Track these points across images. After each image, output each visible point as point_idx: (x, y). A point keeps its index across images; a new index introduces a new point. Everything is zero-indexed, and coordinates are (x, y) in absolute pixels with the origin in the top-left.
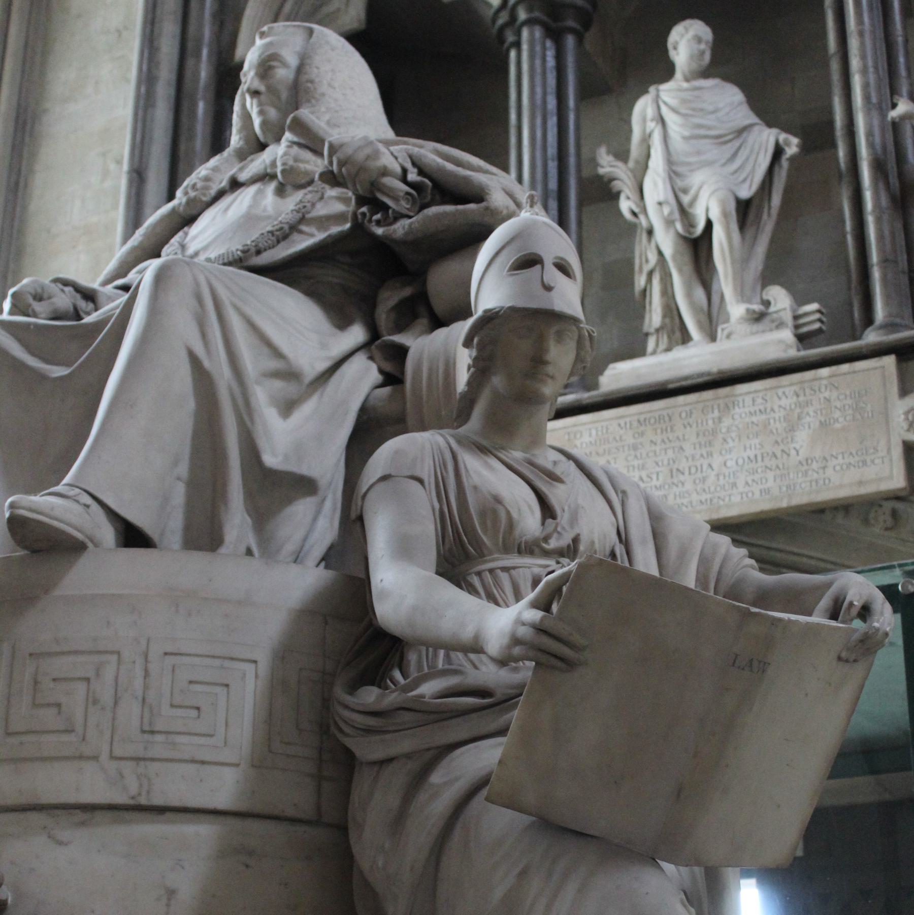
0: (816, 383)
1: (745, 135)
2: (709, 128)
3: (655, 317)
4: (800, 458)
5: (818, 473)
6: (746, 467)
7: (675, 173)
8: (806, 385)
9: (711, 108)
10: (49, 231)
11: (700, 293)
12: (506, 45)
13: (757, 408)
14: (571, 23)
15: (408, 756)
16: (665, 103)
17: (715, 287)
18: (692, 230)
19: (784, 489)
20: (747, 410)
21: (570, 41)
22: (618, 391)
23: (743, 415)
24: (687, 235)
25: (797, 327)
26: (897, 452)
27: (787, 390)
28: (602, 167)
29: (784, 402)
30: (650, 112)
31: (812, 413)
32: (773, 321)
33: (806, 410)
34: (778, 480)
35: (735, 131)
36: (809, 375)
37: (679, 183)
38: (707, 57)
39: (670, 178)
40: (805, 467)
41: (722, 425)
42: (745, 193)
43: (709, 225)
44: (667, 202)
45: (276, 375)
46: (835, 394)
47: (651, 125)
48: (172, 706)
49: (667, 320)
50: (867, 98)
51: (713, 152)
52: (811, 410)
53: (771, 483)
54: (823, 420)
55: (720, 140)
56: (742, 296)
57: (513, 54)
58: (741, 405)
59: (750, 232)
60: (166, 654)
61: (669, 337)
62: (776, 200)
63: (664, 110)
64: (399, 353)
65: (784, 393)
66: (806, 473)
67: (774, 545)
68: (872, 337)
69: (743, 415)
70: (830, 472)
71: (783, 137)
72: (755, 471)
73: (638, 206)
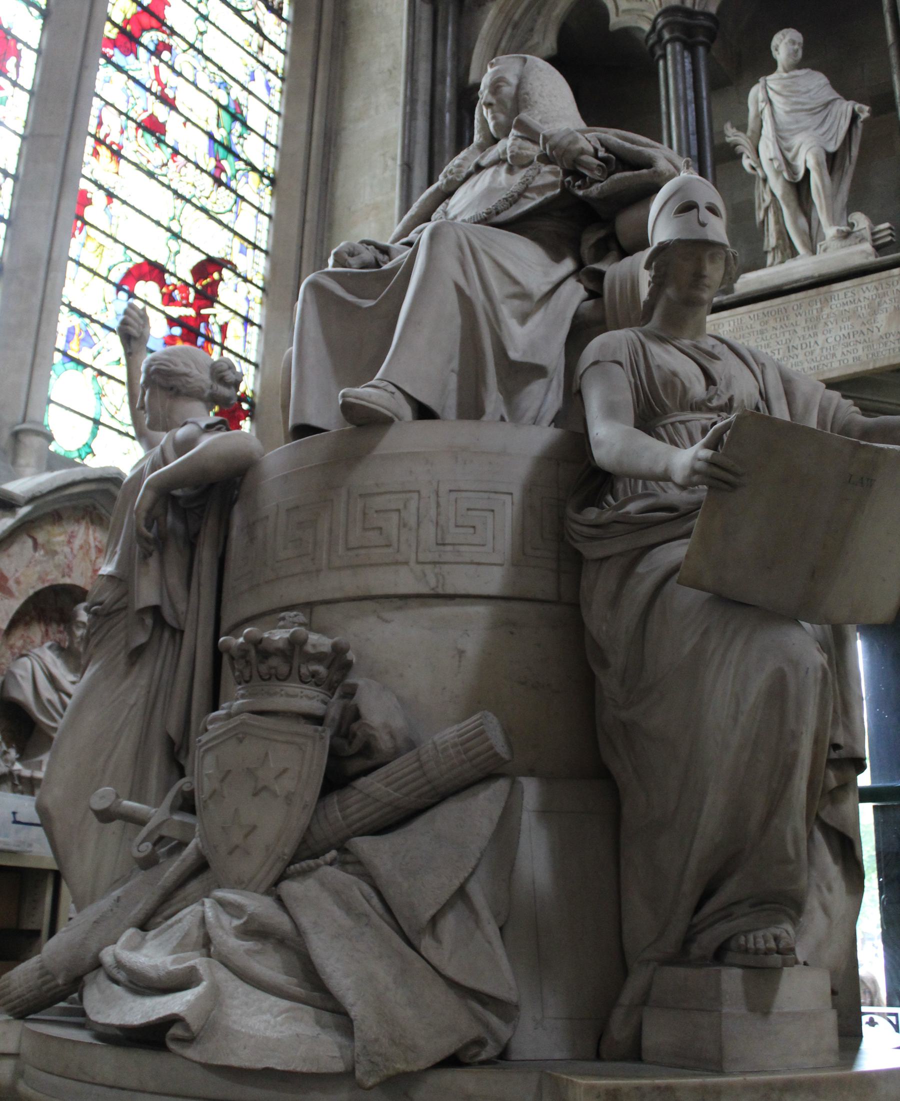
0: (891, 279)
1: (830, 107)
2: (803, 104)
3: (771, 239)
4: (880, 334)
5: (894, 343)
6: (842, 342)
7: (781, 138)
8: (883, 281)
9: (804, 90)
11: (803, 221)
12: (656, 57)
13: (848, 300)
14: (701, 38)
15: (621, 554)
16: (771, 89)
17: (813, 215)
18: (795, 177)
19: (870, 356)
20: (841, 301)
21: (701, 50)
22: (748, 293)
23: (838, 305)
24: (792, 181)
25: (874, 241)
27: (869, 286)
28: (729, 137)
29: (867, 294)
30: (761, 96)
31: (888, 301)
32: (857, 237)
33: (884, 299)
34: (866, 350)
35: (823, 105)
36: (884, 274)
37: (784, 144)
38: (800, 54)
39: (778, 141)
40: (885, 340)
41: (824, 313)
42: (832, 148)
43: (807, 172)
44: (776, 158)
45: (514, 296)
47: (762, 105)
48: (457, 526)
49: (781, 242)
51: (807, 120)
52: (887, 299)
53: (860, 352)
54: (896, 305)
55: (812, 112)
56: (833, 221)
57: (661, 63)
58: (836, 298)
59: (836, 177)
60: (450, 491)
61: (782, 254)
62: (855, 151)
63: (771, 93)
64: (600, 275)
65: (867, 288)
66: (886, 344)
67: (864, 396)
69: (838, 305)
71: (857, 106)
72: (848, 345)
73: (755, 162)
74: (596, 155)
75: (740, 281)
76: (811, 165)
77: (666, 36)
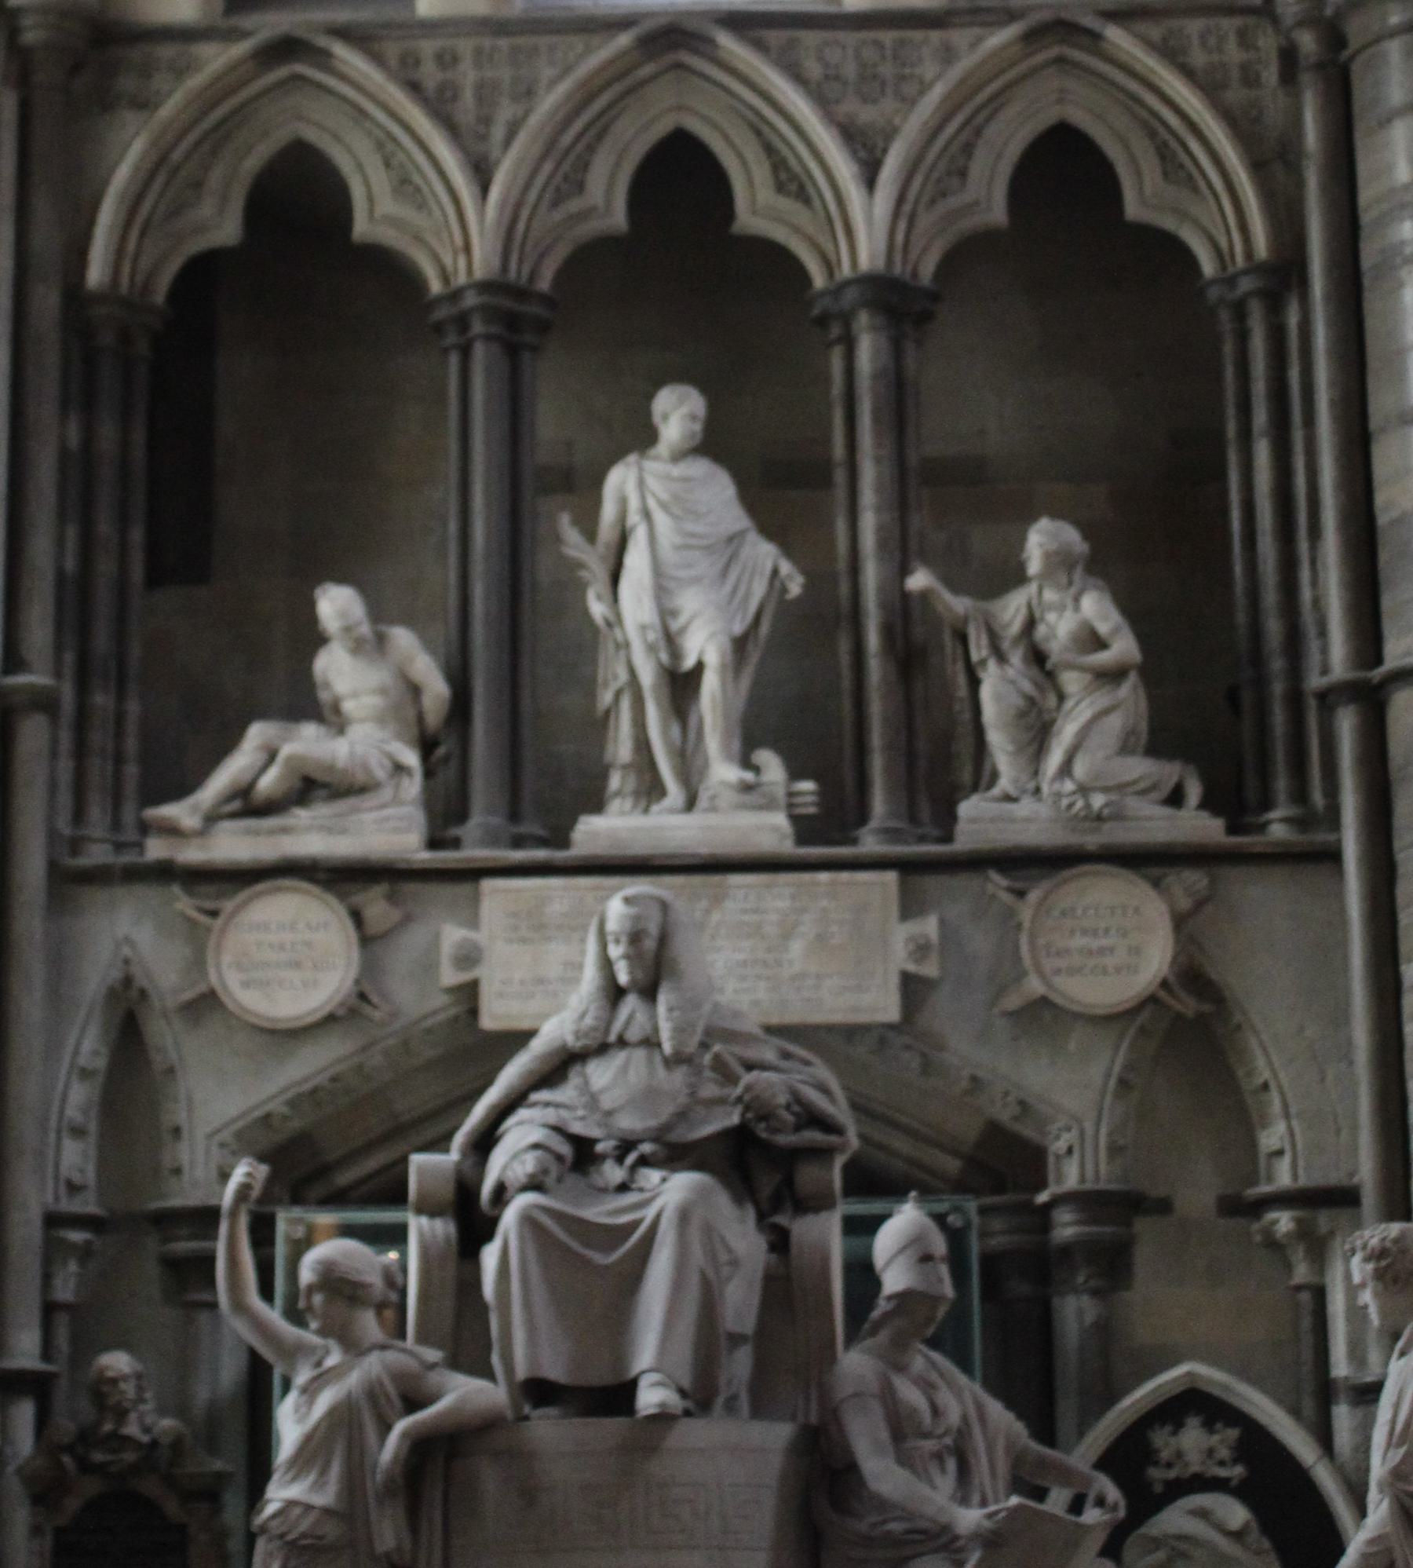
1: (736, 541)
3: (622, 748)
11: (675, 731)
16: (654, 494)
25: (790, 806)
26: (894, 981)
36: (806, 877)
42: (738, 628)
43: (700, 667)
50: (882, 544)
56: (728, 757)
63: (652, 504)
68: (870, 844)
71: (786, 567)
76: (712, 659)
77: (478, 327)
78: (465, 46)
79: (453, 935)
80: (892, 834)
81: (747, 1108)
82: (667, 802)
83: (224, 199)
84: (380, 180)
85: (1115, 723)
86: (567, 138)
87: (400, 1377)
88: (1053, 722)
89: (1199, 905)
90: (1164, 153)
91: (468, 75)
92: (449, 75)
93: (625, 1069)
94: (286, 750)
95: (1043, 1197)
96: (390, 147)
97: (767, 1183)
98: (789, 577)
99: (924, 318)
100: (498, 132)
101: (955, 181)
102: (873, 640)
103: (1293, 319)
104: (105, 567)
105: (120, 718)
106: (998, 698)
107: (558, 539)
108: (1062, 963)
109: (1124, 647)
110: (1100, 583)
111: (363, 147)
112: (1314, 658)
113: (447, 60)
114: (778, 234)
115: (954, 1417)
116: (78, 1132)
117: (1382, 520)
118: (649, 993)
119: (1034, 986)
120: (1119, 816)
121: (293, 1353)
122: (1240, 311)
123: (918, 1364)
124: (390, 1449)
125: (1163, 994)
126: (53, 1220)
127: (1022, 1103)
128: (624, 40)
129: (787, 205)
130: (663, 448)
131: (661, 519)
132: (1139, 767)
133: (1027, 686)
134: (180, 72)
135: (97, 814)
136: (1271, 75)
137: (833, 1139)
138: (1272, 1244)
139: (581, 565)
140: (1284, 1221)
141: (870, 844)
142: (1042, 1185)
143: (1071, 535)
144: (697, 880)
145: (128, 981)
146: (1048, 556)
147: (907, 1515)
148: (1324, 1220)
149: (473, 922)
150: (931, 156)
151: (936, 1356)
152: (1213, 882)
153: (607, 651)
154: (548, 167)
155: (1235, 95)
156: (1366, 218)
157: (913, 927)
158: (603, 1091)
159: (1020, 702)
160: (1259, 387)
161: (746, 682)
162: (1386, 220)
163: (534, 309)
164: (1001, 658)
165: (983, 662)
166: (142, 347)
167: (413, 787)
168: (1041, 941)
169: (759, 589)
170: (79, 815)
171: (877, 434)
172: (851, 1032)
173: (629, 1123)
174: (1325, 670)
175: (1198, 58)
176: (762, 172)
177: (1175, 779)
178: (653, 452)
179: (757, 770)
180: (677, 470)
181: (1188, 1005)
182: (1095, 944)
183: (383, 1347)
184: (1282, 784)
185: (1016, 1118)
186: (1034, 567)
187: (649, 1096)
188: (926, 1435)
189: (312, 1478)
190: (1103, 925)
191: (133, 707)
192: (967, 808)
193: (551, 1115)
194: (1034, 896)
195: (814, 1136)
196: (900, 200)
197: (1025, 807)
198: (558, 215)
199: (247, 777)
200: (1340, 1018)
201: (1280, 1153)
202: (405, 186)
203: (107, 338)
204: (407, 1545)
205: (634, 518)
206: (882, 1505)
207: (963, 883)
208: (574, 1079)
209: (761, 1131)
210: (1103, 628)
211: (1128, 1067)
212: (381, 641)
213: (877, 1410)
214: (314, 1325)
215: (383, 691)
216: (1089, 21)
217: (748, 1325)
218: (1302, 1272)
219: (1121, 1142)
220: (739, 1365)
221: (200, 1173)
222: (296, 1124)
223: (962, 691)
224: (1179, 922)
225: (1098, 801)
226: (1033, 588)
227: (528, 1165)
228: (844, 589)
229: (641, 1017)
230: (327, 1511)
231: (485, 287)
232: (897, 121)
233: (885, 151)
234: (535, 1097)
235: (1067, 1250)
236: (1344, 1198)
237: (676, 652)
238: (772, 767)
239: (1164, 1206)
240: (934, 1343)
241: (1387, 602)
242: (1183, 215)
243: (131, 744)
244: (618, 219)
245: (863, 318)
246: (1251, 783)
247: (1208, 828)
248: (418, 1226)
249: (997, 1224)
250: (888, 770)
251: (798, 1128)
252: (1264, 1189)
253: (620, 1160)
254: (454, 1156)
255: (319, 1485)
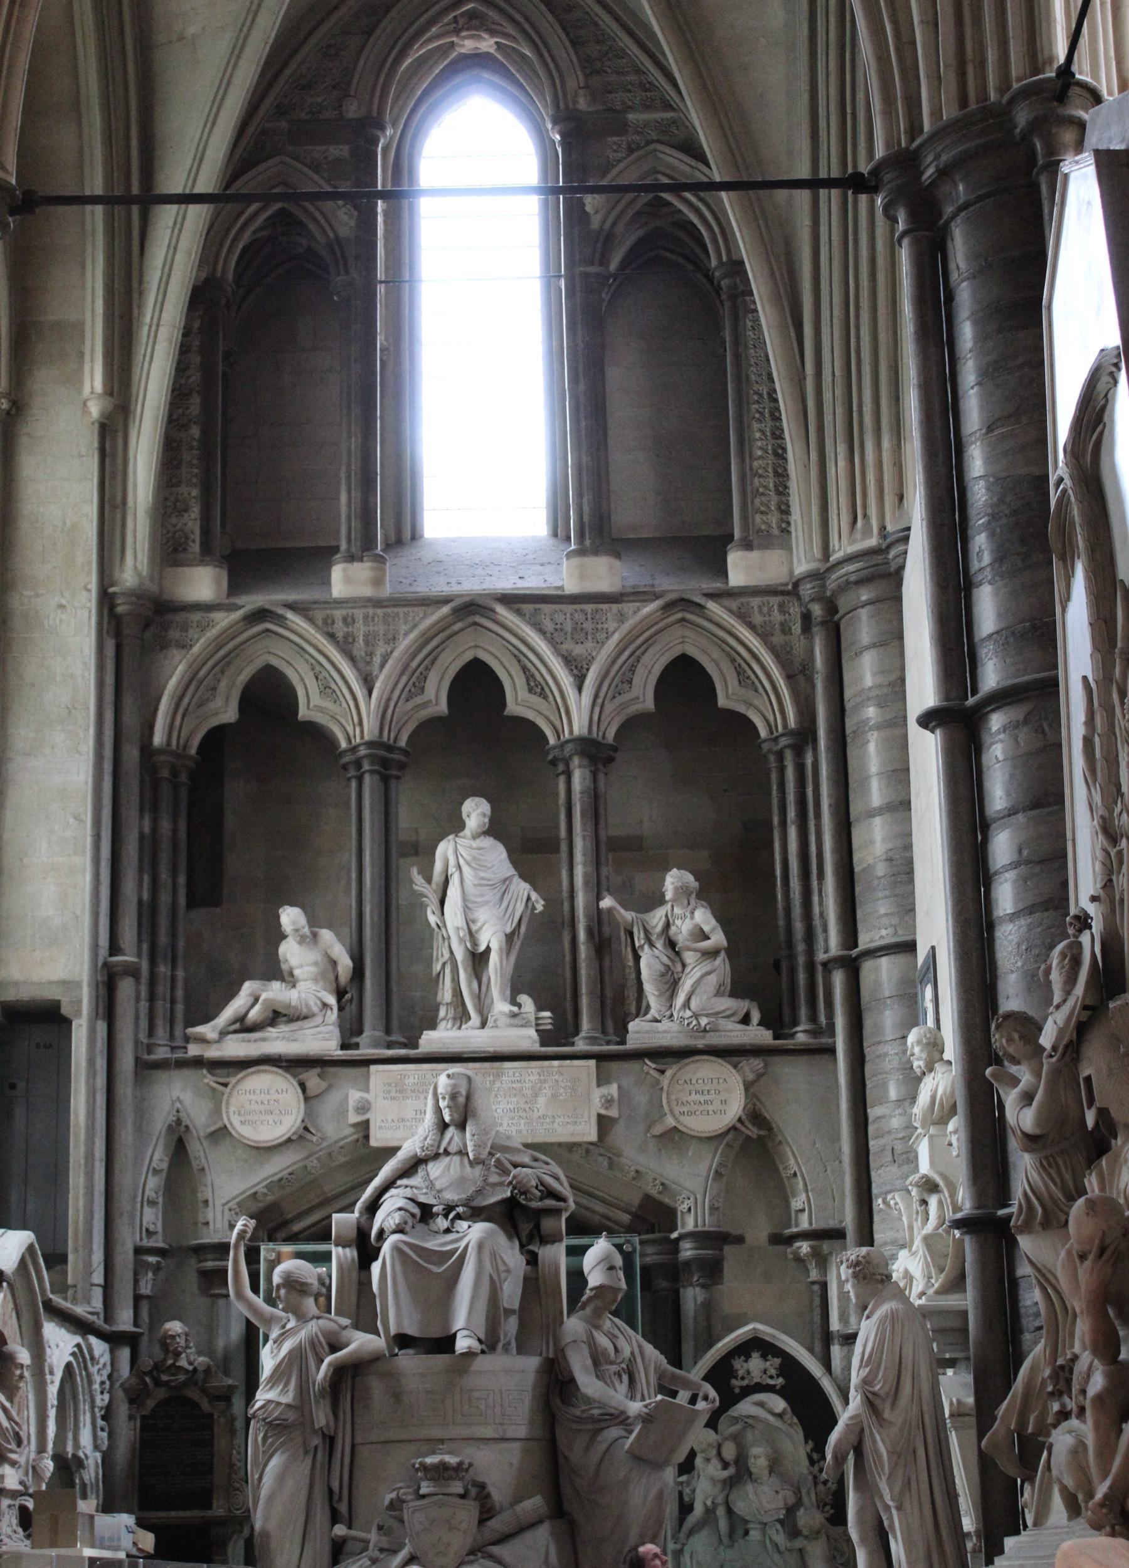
2: (489, 880)
3: (446, 994)
10: (21, 860)
11: (475, 985)
17: (484, 979)
25: (537, 1025)
26: (594, 1120)
29: (531, 1078)
36: (546, 1063)
37: (470, 916)
42: (509, 930)
43: (488, 949)
46: (561, 1078)
50: (586, 883)
52: (547, 1086)
66: (542, 1124)
68: (581, 1045)
70: (556, 1125)
71: (534, 896)
72: (513, 1118)
74: (537, 1187)
75: (423, 1037)
76: (495, 946)
77: (366, 766)
78: (359, 613)
79: (355, 1096)
80: (592, 1040)
81: (514, 1188)
82: (470, 1023)
83: (228, 698)
84: (313, 686)
85: (713, 979)
86: (414, 664)
87: (328, 1334)
88: (679, 979)
89: (759, 1076)
90: (739, 672)
91: (360, 629)
92: (351, 629)
93: (448, 1168)
94: (264, 996)
95: (674, 1235)
96: (318, 668)
97: (525, 1228)
98: (537, 901)
99: (610, 760)
100: (377, 660)
101: (626, 686)
102: (582, 935)
103: (809, 761)
104: (165, 898)
105: (173, 978)
106: (650, 966)
107: (411, 882)
108: (685, 1109)
109: (718, 938)
110: (705, 904)
111: (303, 668)
112: (820, 944)
113: (348, 621)
114: (530, 715)
115: (626, 1352)
116: (152, 1203)
117: (857, 870)
118: (462, 1126)
119: (670, 1121)
120: (715, 1030)
121: (269, 1321)
122: (780, 756)
123: (607, 1325)
124: (323, 1371)
125: (739, 1125)
126: (139, 1251)
127: (663, 1184)
128: (445, 609)
129: (534, 699)
130: (467, 832)
131: (465, 868)
132: (726, 1003)
133: (665, 960)
134: (203, 628)
135: (161, 1032)
136: (797, 628)
137: (562, 1204)
138: (798, 1259)
139: (423, 895)
140: (804, 1247)
141: (581, 1045)
142: (675, 1228)
143: (689, 878)
144: (487, 1065)
145: (179, 1122)
146: (676, 889)
147: (602, 1405)
148: (826, 1246)
149: (367, 1090)
150: (612, 673)
151: (616, 1320)
152: (766, 1065)
153: (438, 942)
154: (404, 679)
155: (778, 639)
156: (848, 706)
157: (604, 1090)
158: (436, 1179)
159: (662, 969)
160: (791, 798)
161: (513, 959)
162: (858, 707)
163: (396, 756)
164: (652, 945)
165: (642, 947)
166: (184, 778)
167: (333, 1016)
168: (673, 1097)
169: (520, 908)
170: (151, 1032)
171: (584, 824)
172: (571, 1147)
173: (451, 1196)
174: (826, 951)
175: (757, 619)
176: (520, 682)
177: (745, 1010)
178: (461, 834)
179: (520, 1006)
180: (474, 844)
181: (753, 1131)
182: (702, 1098)
183: (318, 1318)
184: (803, 1012)
185: (660, 1193)
186: (669, 896)
187: (462, 1181)
188: (612, 1363)
189: (281, 1387)
190: (707, 1088)
191: (180, 974)
192: (632, 1026)
193: (408, 1192)
194: (669, 1073)
195: (550, 1203)
196: (596, 696)
197: (665, 1025)
198: (410, 705)
199: (244, 1011)
200: (835, 1138)
201: (803, 1210)
202: (326, 689)
203: (165, 773)
204: (332, 1424)
205: (452, 869)
206: (588, 1400)
207: (633, 1066)
208: (421, 1172)
209: (522, 1200)
210: (706, 928)
211: (720, 1164)
212: (315, 935)
213: (585, 1347)
214: (281, 1306)
215: (316, 964)
216: (698, 599)
217: (516, 1305)
218: (814, 1275)
219: (716, 1205)
220: (511, 1326)
221: (219, 1224)
222: (270, 1198)
223: (631, 963)
224: (748, 1086)
225: (704, 1021)
226: (669, 906)
227: (397, 1218)
228: (566, 907)
229: (456, 1139)
230: (288, 1406)
231: (370, 744)
232: (594, 654)
233: (588, 670)
234: (399, 1182)
235: (687, 1263)
236: (837, 1234)
237: (475, 943)
238: (527, 1003)
239: (740, 1240)
240: (615, 1313)
241: (860, 913)
242: (750, 705)
243: (180, 993)
244: (443, 707)
245: (576, 761)
246: (786, 1011)
247: (762, 1036)
248: (337, 1252)
249: (650, 1250)
250: (589, 1006)
251: (541, 1199)
252: (795, 1230)
253: (446, 1216)
254: (356, 1214)
255: (284, 1391)
